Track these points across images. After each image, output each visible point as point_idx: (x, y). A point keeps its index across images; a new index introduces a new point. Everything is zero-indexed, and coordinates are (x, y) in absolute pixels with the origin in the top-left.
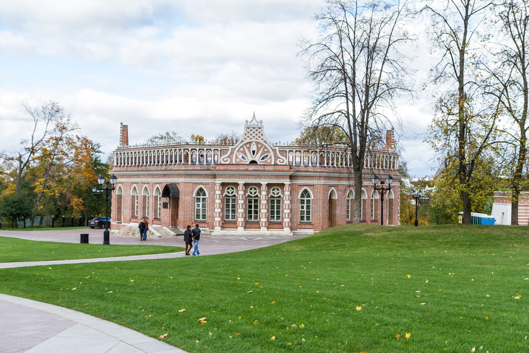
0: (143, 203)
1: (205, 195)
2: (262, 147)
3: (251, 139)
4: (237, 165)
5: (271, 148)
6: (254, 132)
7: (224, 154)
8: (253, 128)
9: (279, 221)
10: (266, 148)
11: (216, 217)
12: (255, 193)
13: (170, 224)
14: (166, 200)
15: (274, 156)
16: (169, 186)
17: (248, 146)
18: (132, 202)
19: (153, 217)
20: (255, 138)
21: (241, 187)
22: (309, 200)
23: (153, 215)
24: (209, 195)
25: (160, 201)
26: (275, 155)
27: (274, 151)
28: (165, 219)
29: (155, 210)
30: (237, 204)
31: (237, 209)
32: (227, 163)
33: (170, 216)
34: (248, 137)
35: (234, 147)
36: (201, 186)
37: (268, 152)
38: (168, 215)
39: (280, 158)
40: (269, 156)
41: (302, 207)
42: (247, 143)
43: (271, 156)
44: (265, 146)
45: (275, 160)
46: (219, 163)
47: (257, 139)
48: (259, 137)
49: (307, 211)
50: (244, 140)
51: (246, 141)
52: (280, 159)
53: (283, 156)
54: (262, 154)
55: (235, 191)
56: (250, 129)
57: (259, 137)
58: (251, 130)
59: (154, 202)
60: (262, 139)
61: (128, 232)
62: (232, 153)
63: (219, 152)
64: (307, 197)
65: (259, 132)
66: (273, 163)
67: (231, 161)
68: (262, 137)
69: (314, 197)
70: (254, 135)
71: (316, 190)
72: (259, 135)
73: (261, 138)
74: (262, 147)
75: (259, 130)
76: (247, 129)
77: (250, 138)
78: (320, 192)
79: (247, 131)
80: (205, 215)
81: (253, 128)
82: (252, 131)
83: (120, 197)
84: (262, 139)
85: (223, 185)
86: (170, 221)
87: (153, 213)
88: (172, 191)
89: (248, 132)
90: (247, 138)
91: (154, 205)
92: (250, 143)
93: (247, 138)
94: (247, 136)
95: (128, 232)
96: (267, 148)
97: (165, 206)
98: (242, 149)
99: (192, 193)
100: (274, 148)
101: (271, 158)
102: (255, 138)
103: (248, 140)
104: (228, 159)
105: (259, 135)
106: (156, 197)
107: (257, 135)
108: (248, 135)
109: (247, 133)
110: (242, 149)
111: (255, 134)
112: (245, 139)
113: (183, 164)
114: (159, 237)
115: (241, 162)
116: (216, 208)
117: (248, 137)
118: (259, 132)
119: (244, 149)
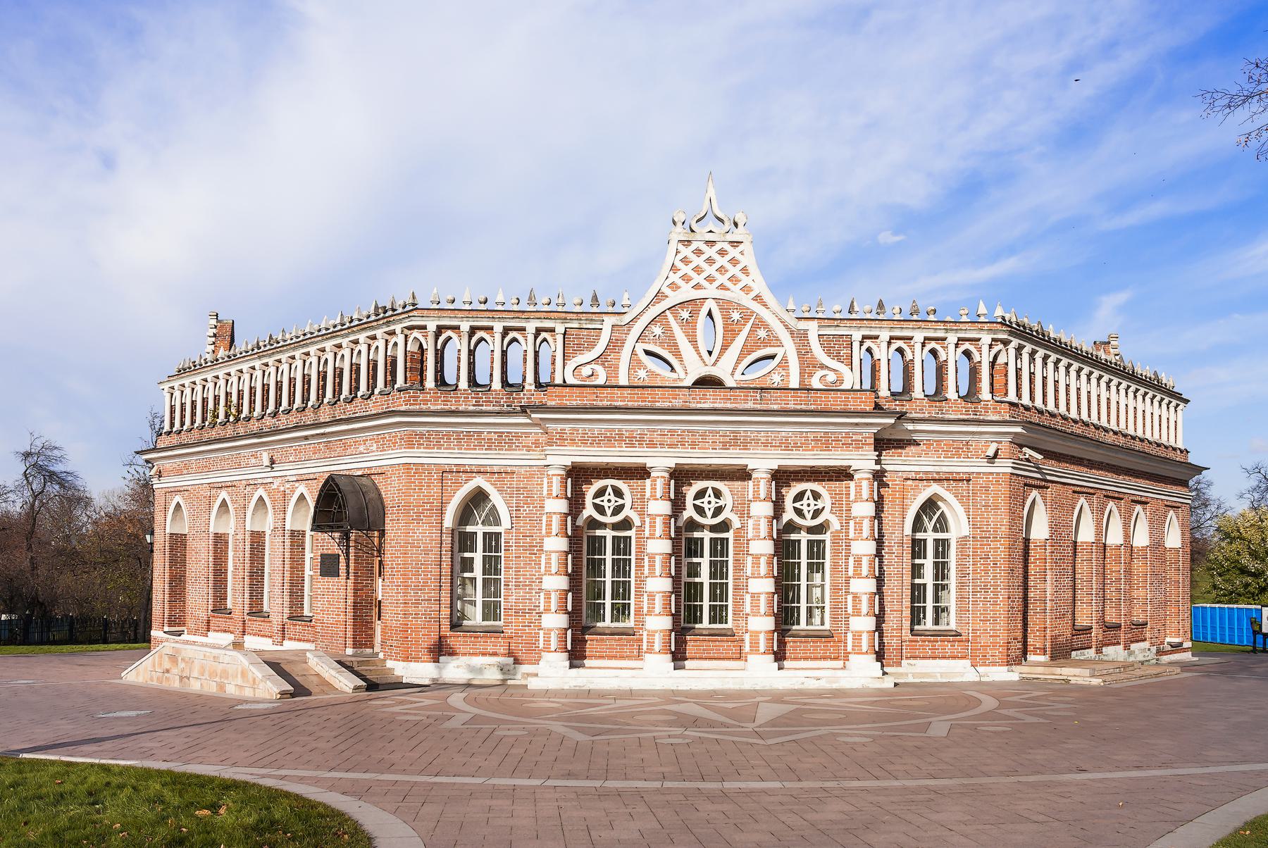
0: (252, 561)
1: (497, 522)
2: (745, 319)
3: (697, 286)
5: (787, 327)
8: (707, 242)
9: (810, 627)
10: (760, 324)
11: (547, 610)
12: (718, 511)
13: (349, 642)
14: (330, 543)
17: (685, 315)
18: (215, 558)
19: (287, 610)
20: (717, 284)
23: (287, 604)
24: (515, 518)
27: (801, 338)
28: (329, 619)
29: (292, 585)
30: (640, 560)
31: (641, 581)
33: (350, 609)
34: (686, 278)
36: (479, 481)
37: (773, 340)
38: (342, 605)
39: (823, 367)
40: (777, 360)
41: (916, 571)
43: (785, 359)
44: (758, 317)
48: (734, 279)
51: (674, 298)
53: (838, 357)
54: (745, 351)
55: (627, 500)
59: (287, 555)
60: (747, 289)
61: (168, 671)
62: (615, 345)
64: (935, 530)
65: (734, 262)
66: (794, 383)
70: (710, 270)
71: (981, 498)
72: (733, 271)
74: (747, 320)
75: (733, 252)
76: (681, 247)
77: (692, 283)
79: (680, 256)
80: (497, 605)
83: (178, 543)
84: (747, 289)
86: (349, 628)
87: (287, 598)
88: (352, 502)
89: (685, 261)
91: (287, 567)
92: (693, 305)
95: (168, 671)
96: (766, 326)
97: (329, 566)
99: (442, 513)
101: (784, 364)
102: (717, 284)
103: (686, 293)
104: (600, 370)
105: (733, 271)
106: (297, 538)
107: (721, 270)
109: (679, 264)
110: (657, 330)
112: (674, 286)
116: (550, 494)
117: (686, 278)
118: (734, 262)
119: (667, 329)
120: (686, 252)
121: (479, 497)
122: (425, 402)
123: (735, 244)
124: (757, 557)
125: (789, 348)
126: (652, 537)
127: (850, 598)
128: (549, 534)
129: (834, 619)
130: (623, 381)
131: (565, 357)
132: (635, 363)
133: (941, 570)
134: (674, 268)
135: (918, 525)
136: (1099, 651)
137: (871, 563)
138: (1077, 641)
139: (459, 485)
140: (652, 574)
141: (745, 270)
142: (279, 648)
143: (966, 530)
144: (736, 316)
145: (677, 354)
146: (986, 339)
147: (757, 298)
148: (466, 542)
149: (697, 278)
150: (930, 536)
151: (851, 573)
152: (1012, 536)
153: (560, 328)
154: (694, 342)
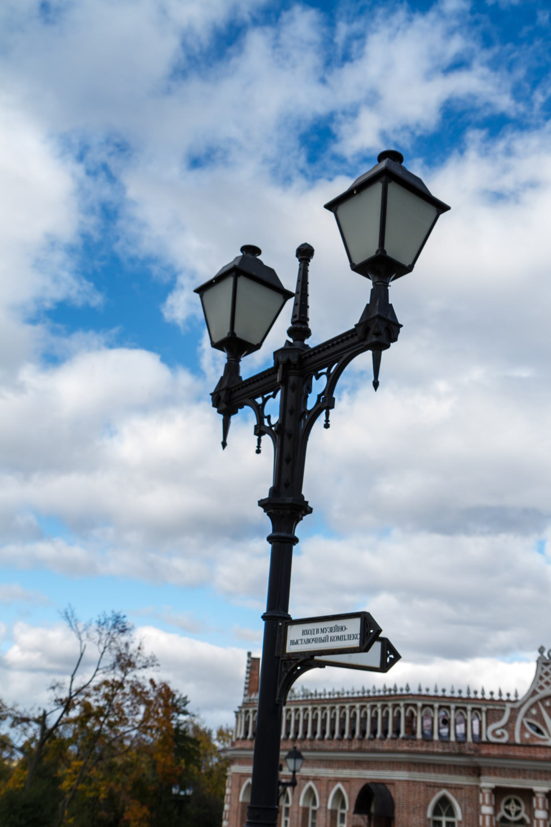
32: (504, 740)
50: (538, 690)
62: (513, 719)
67: (512, 736)
76: (544, 667)
79: (544, 671)
90: (544, 686)
93: (544, 686)
94: (544, 681)
98: (534, 712)
110: (534, 712)
112: (541, 688)
119: (539, 710)
121: (444, 802)
122: (417, 746)
131: (487, 725)
132: (523, 729)
139: (434, 794)
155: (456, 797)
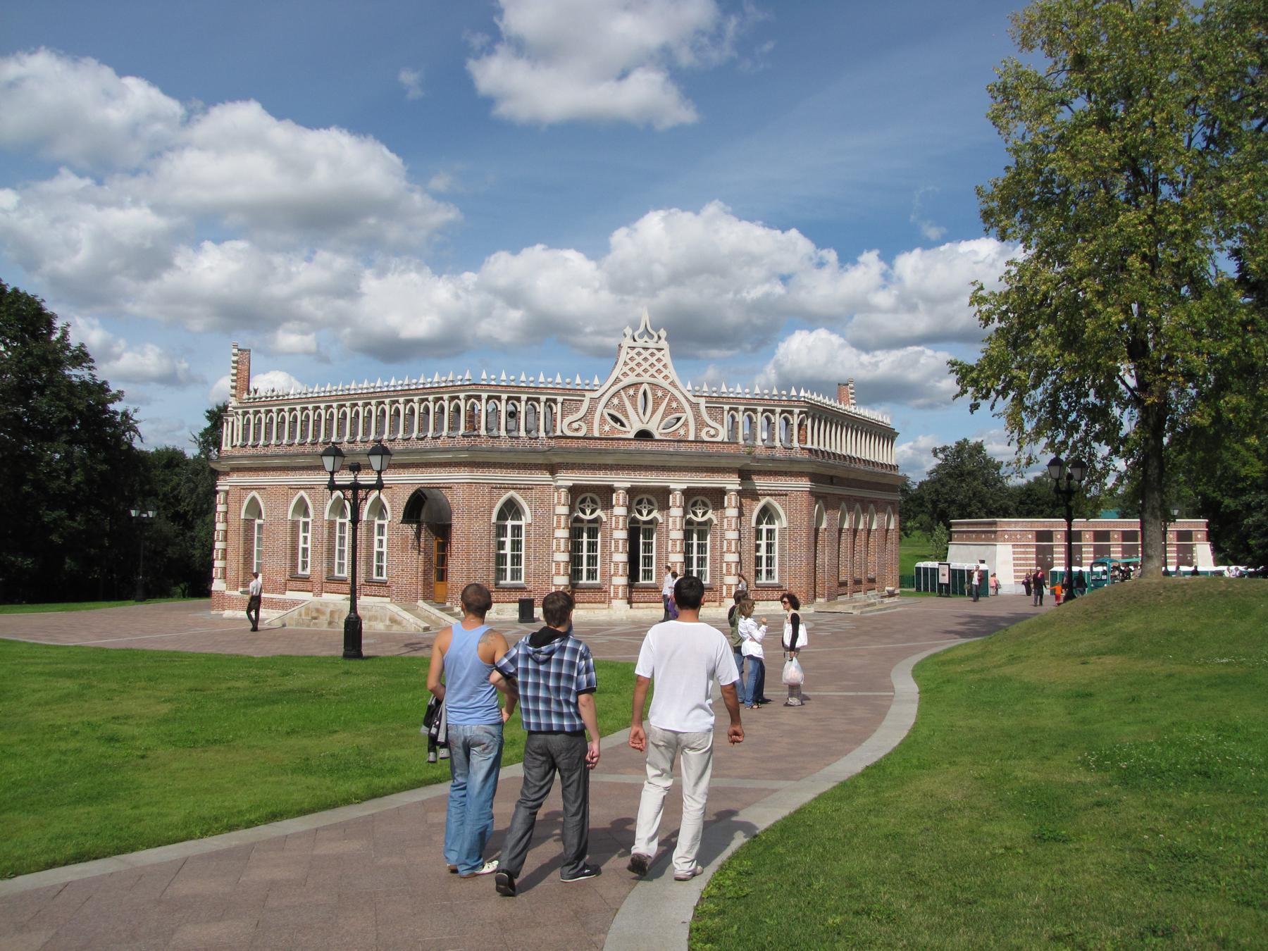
2: (664, 396)
3: (638, 375)
4: (607, 439)
5: (688, 400)
6: (645, 359)
7: (571, 412)
8: (644, 348)
10: (674, 398)
15: (695, 419)
16: (425, 491)
17: (631, 392)
20: (649, 374)
21: (619, 498)
22: (519, 527)
25: (304, 532)
26: (697, 416)
32: (581, 434)
34: (632, 370)
35: (596, 395)
37: (680, 409)
42: (630, 386)
43: (686, 420)
45: (696, 429)
46: (558, 433)
47: (652, 376)
48: (659, 371)
49: (513, 556)
52: (709, 429)
53: (715, 420)
54: (665, 415)
56: (650, 351)
57: (659, 371)
58: (639, 354)
60: (666, 377)
61: (315, 618)
62: (591, 410)
63: (559, 405)
65: (659, 360)
67: (590, 429)
68: (665, 372)
69: (535, 516)
70: (646, 365)
72: (659, 366)
73: (663, 375)
74: (666, 396)
75: (659, 355)
76: (629, 350)
77: (636, 373)
78: (801, 511)
79: (629, 356)
81: (644, 348)
82: (642, 357)
84: (666, 377)
85: (574, 491)
90: (629, 372)
92: (636, 385)
93: (629, 372)
94: (629, 367)
95: (315, 618)
96: (676, 400)
98: (616, 401)
100: (694, 400)
101: (686, 424)
102: (649, 374)
103: (632, 379)
105: (659, 366)
107: (652, 365)
108: (633, 364)
109: (629, 361)
110: (616, 401)
111: (649, 363)
112: (625, 374)
113: (463, 436)
114: (426, 629)
115: (613, 433)
117: (632, 370)
118: (659, 360)
119: (621, 400)
120: (633, 353)
123: (659, 350)
124: (674, 541)
125: (689, 414)
126: (617, 528)
127: (724, 565)
128: (559, 527)
129: (713, 577)
130: (596, 434)
133: (770, 547)
134: (625, 364)
135: (759, 522)
136: (851, 596)
137: (736, 544)
138: (841, 590)
140: (617, 550)
141: (665, 366)
142: (316, 599)
143: (785, 524)
144: (660, 394)
145: (627, 417)
146: (797, 411)
147: (672, 383)
148: (501, 530)
149: (639, 370)
150: (764, 527)
151: (725, 549)
152: (809, 527)
153: (560, 399)
154: (636, 409)
155: (525, 499)
